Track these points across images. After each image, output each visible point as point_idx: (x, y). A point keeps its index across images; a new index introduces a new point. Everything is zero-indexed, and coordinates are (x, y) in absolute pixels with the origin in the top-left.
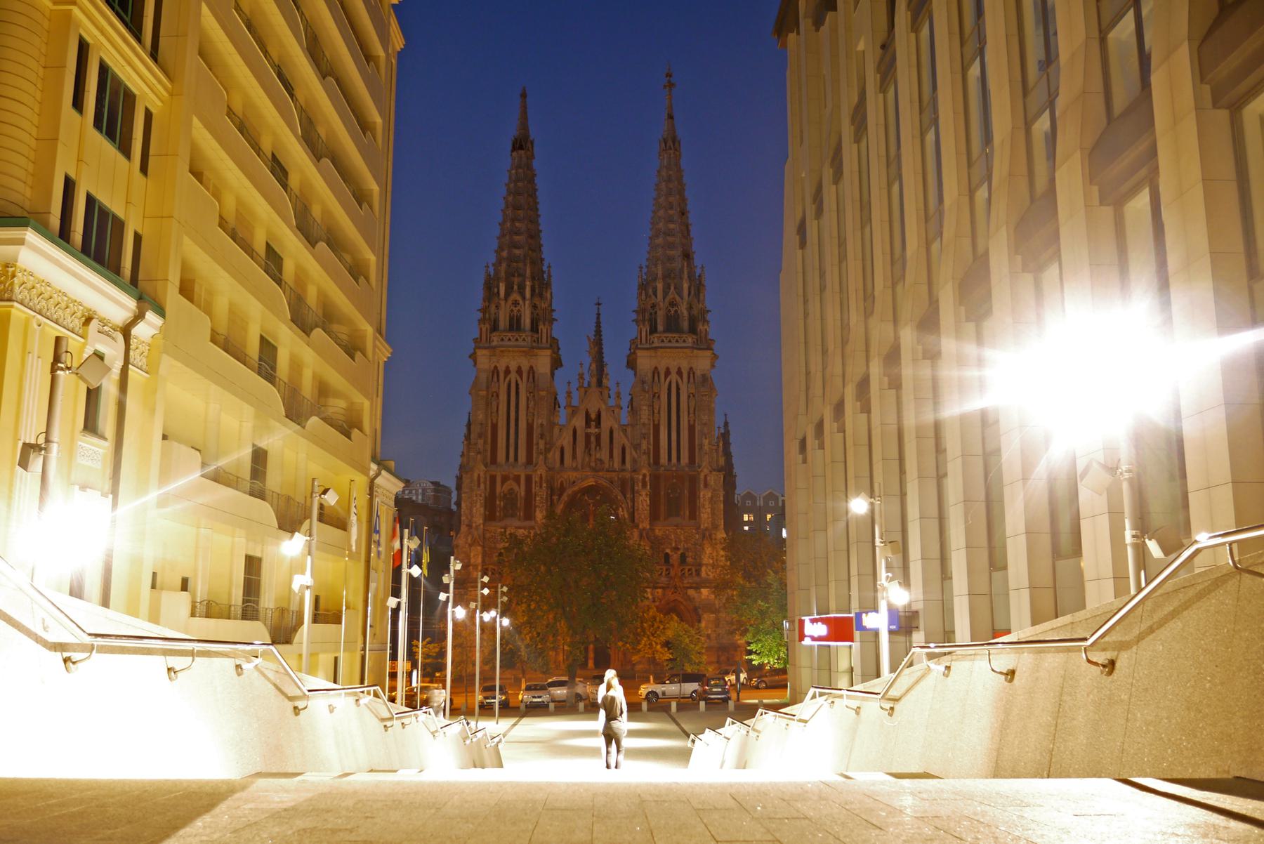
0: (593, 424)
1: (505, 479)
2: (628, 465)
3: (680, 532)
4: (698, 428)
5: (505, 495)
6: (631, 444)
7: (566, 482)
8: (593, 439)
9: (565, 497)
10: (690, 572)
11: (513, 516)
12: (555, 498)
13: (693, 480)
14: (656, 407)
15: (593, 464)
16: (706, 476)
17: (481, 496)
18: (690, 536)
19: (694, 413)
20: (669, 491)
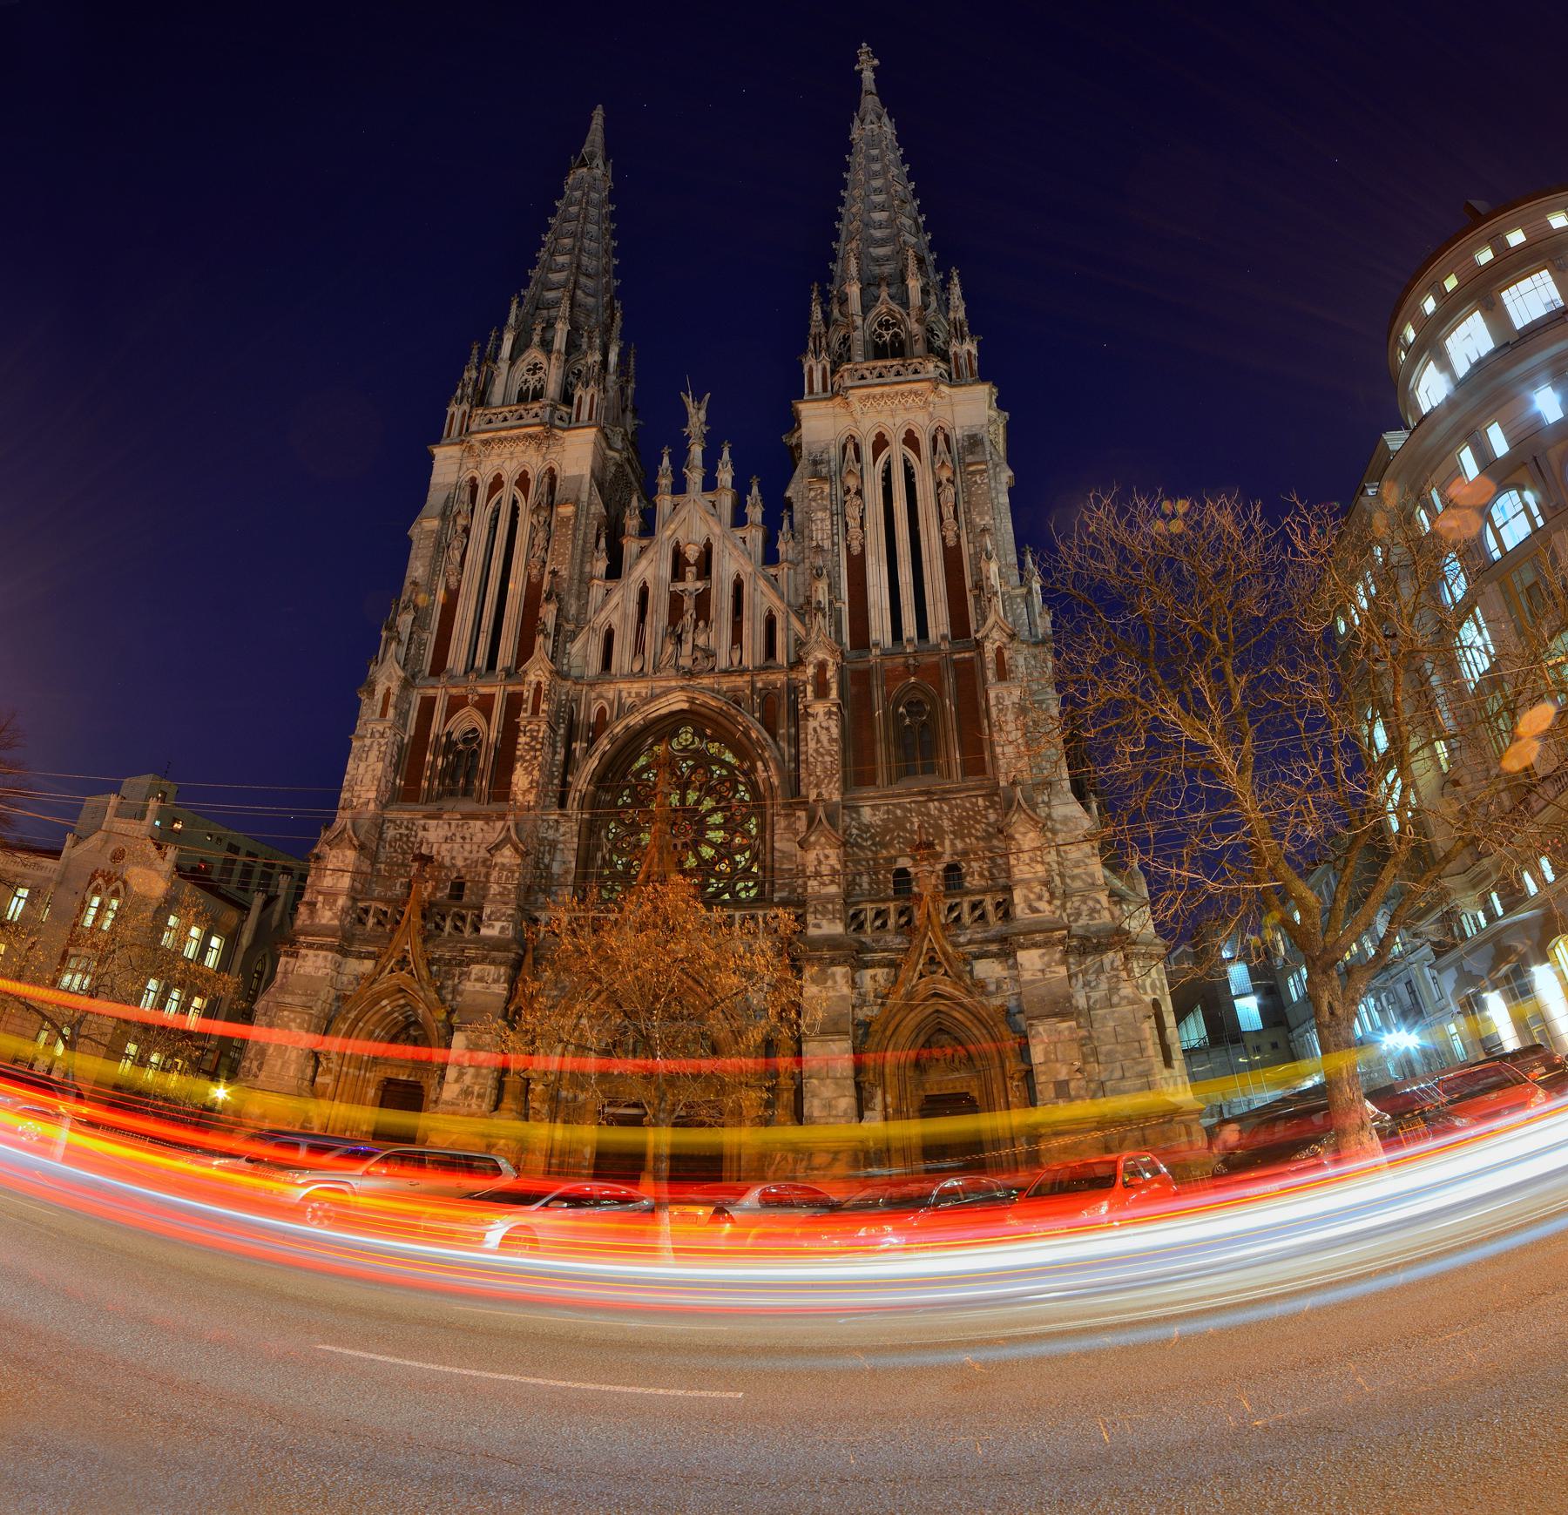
0: (691, 572)
1: (455, 705)
2: (781, 657)
3: (941, 810)
4: (967, 550)
5: (451, 744)
6: (789, 605)
7: (612, 709)
8: (689, 604)
9: (604, 744)
10: (977, 913)
11: (467, 792)
12: (578, 746)
13: (969, 681)
14: (853, 511)
15: (686, 662)
16: (999, 651)
17: (382, 735)
18: (968, 818)
19: (956, 518)
20: (901, 709)
